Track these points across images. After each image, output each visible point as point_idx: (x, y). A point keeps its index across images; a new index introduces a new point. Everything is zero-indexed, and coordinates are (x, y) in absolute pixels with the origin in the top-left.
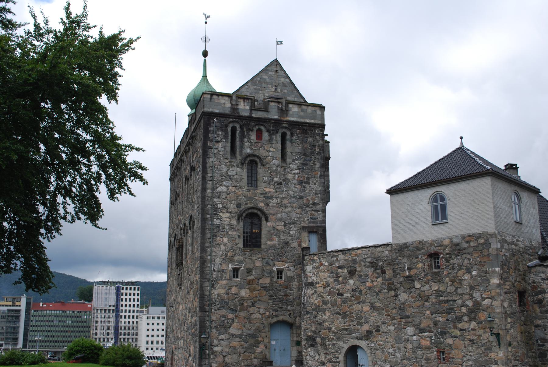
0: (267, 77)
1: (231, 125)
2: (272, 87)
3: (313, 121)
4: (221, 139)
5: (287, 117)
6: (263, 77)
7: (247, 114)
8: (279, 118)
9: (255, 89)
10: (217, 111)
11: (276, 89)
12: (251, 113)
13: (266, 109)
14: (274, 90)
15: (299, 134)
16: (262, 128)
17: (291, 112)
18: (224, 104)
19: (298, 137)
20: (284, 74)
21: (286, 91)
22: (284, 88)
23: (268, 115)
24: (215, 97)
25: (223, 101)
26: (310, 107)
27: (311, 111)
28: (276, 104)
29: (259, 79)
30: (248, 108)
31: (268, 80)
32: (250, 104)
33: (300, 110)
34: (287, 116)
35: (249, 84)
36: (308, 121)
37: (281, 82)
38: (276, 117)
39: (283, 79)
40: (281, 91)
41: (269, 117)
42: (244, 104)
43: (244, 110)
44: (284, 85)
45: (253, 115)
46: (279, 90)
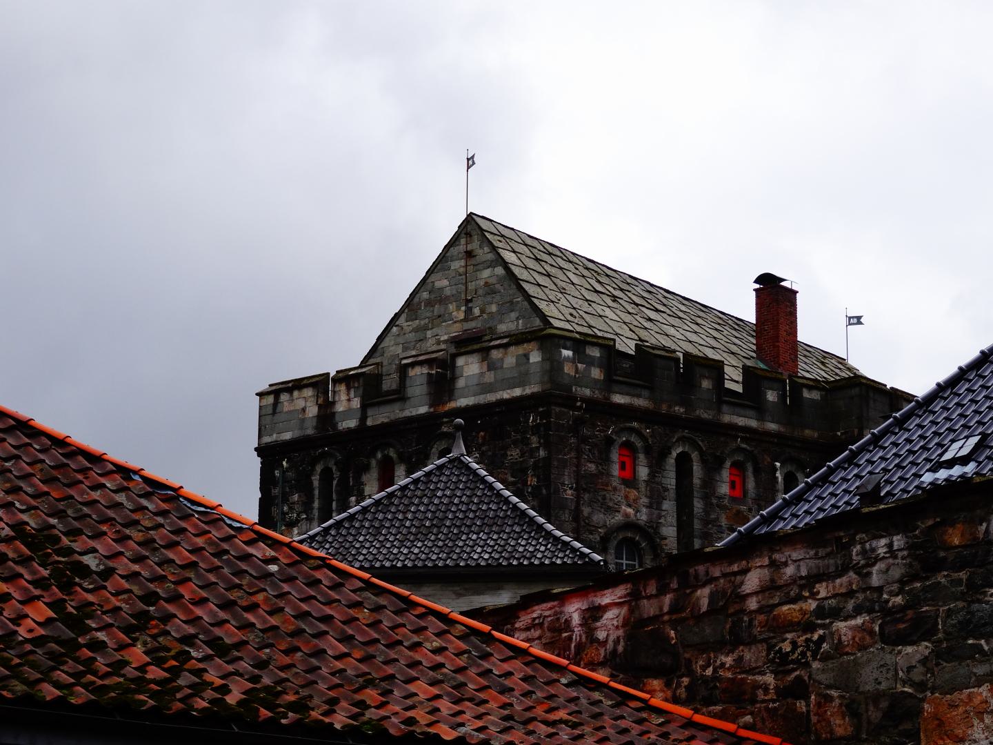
0: (445, 282)
1: (319, 468)
2: (458, 308)
3: (517, 392)
4: (298, 515)
5: (450, 400)
6: (438, 284)
7: (352, 423)
8: (432, 410)
9: (416, 330)
10: (287, 436)
11: (469, 311)
12: (363, 418)
13: (400, 395)
14: (462, 316)
15: (483, 444)
16: (392, 453)
17: (461, 383)
18: (304, 410)
19: (483, 452)
20: (491, 256)
21: (494, 308)
22: (489, 298)
23: (402, 410)
24: (284, 397)
25: (300, 404)
26: (512, 349)
27: (514, 360)
28: (425, 370)
29: (425, 295)
30: (356, 403)
31: (448, 292)
32: (361, 391)
33: (485, 364)
34: (451, 397)
35: (401, 321)
36: (506, 395)
37: (482, 283)
38: (423, 410)
39: (486, 273)
40: (482, 311)
41: (407, 413)
42: (348, 394)
43: (348, 414)
44: (490, 290)
45: (369, 423)
46: (477, 311)
